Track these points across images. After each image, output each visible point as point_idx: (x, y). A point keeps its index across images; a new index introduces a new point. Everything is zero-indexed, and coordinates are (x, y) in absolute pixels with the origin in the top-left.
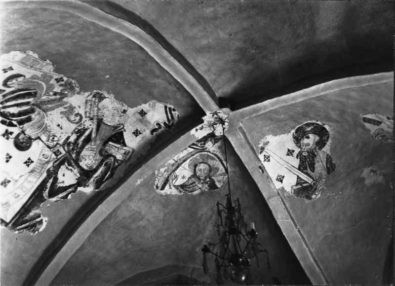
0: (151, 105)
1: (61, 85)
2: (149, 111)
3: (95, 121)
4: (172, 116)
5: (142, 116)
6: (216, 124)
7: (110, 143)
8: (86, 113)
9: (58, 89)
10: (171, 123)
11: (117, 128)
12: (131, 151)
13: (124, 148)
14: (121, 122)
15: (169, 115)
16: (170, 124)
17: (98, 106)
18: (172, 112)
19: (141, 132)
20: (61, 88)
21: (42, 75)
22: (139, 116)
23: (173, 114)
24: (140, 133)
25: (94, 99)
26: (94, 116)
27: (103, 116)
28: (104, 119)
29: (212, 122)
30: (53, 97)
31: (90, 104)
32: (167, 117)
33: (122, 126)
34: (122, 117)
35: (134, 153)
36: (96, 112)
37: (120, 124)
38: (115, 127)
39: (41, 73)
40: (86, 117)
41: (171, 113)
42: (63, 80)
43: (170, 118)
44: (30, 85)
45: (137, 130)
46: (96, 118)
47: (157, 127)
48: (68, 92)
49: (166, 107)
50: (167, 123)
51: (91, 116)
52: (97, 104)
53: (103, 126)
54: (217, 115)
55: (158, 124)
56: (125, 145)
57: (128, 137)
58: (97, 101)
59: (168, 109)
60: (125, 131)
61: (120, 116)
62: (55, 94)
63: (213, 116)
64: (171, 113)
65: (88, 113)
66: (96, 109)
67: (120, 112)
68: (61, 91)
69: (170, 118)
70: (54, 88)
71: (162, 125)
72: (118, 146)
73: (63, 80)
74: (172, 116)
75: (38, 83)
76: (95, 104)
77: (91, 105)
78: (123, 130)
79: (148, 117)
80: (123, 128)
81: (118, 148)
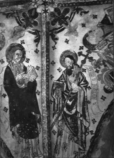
0: (77, 26)
1: (100, 68)
2: (79, 24)
3: (106, 38)
4: (71, 14)
5: (85, 24)
6: (50, 3)
7: (111, 22)
8: (105, 45)
9: (102, 67)
10: (74, 11)
11: (101, 26)
12: (106, 10)
13: (108, 14)
14: (97, 27)
15: (72, 16)
16: (75, 11)
17: (98, 43)
18: (69, 16)
19: (93, 16)
20: (101, 66)
21: (99, 80)
22: (86, 25)
23: (70, 15)
24: (94, 15)
25: (96, 48)
26: (104, 41)
27: (101, 37)
28: (102, 35)
29: (51, 5)
30: (108, 65)
31: (100, 48)
32: (74, 16)
33: (98, 25)
34: (94, 30)
35: (105, 8)
36: (102, 42)
37: (98, 27)
38: (102, 27)
39: (99, 81)
40: (108, 43)
41: (71, 16)
42: (97, 70)
43: (73, 14)
44: (108, 80)
45: (94, 18)
46: (104, 39)
47: (83, 13)
48: (101, 62)
49: (71, 21)
50: (76, 13)
51: (105, 41)
52: (98, 45)
53: (106, 33)
54: (45, 10)
55: (81, 15)
56: (106, 15)
57: (100, 19)
58: (96, 46)
59: (71, 19)
60: (99, 22)
61: (95, 31)
62: (105, 66)
63: (48, 10)
64: (71, 16)
65: (105, 44)
66: (100, 43)
67: (93, 32)
68: (102, 65)
69: (73, 14)
70: (104, 69)
71: (80, 13)
72: (109, 17)
73: (97, 70)
74: (71, 14)
75: (105, 78)
76: (98, 46)
77: (100, 47)
78: (100, 23)
79: (83, 22)
80: (99, 24)
81: (110, 16)
